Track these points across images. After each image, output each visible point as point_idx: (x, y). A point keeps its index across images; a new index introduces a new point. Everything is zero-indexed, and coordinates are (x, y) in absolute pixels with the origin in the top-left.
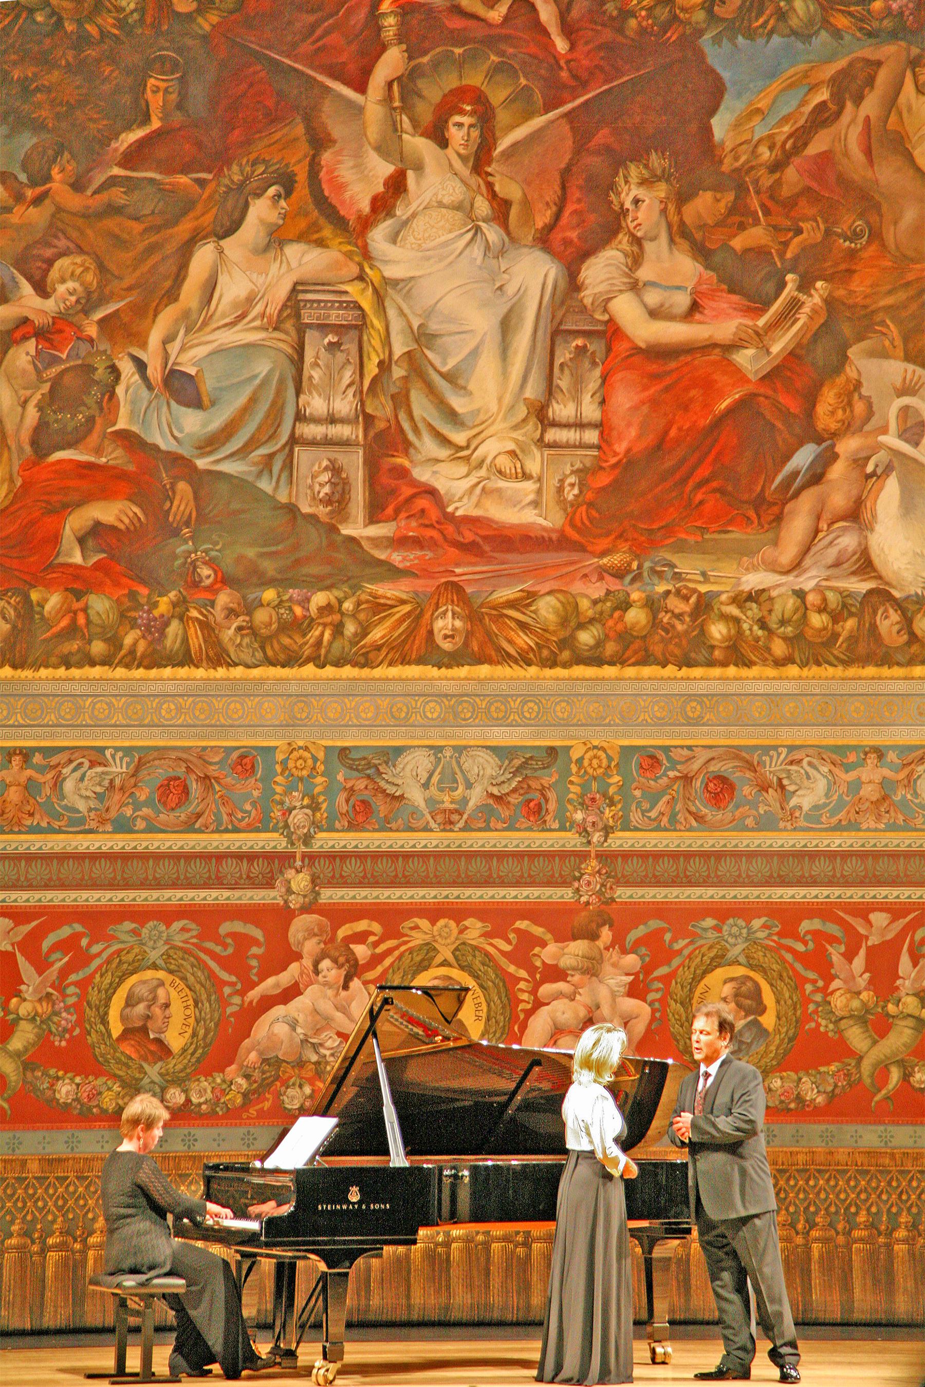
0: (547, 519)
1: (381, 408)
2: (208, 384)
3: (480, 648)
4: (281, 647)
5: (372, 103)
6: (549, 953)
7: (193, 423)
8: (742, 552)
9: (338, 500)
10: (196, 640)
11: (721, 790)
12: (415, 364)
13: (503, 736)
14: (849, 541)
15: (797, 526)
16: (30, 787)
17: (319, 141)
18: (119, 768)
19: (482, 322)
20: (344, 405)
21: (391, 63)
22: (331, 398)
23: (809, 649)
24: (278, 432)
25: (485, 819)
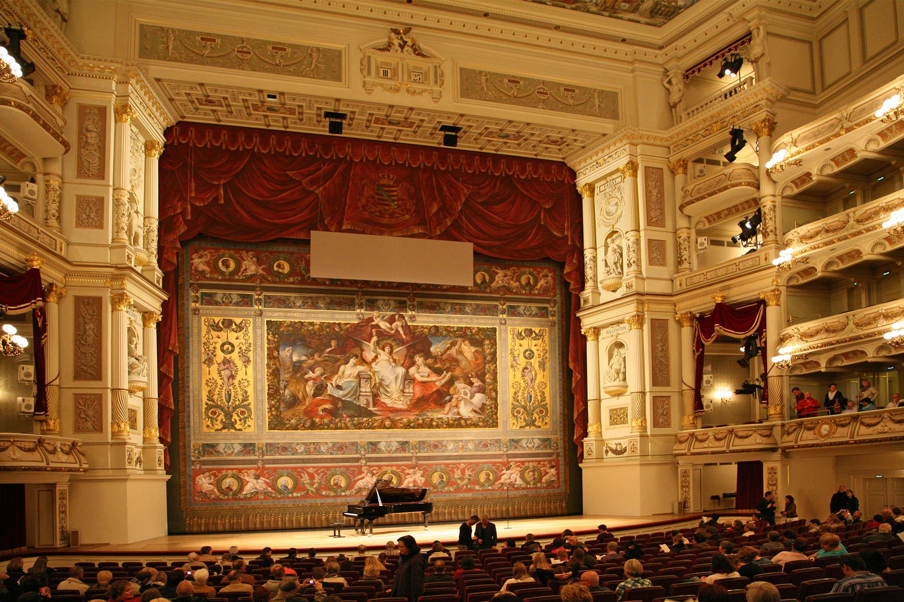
0: (405, 407)
1: (375, 391)
2: (344, 387)
3: (394, 425)
4: (358, 426)
5: (371, 345)
6: (407, 471)
7: (341, 393)
8: (438, 412)
9: (368, 404)
10: (343, 425)
11: (436, 447)
12: (381, 384)
13: (398, 439)
14: (456, 410)
15: (447, 407)
16: (315, 448)
17: (362, 350)
18: (330, 445)
19: (392, 378)
20: (368, 390)
21: (375, 339)
22: (366, 388)
23: (449, 426)
24: (356, 392)
25: (396, 451)
